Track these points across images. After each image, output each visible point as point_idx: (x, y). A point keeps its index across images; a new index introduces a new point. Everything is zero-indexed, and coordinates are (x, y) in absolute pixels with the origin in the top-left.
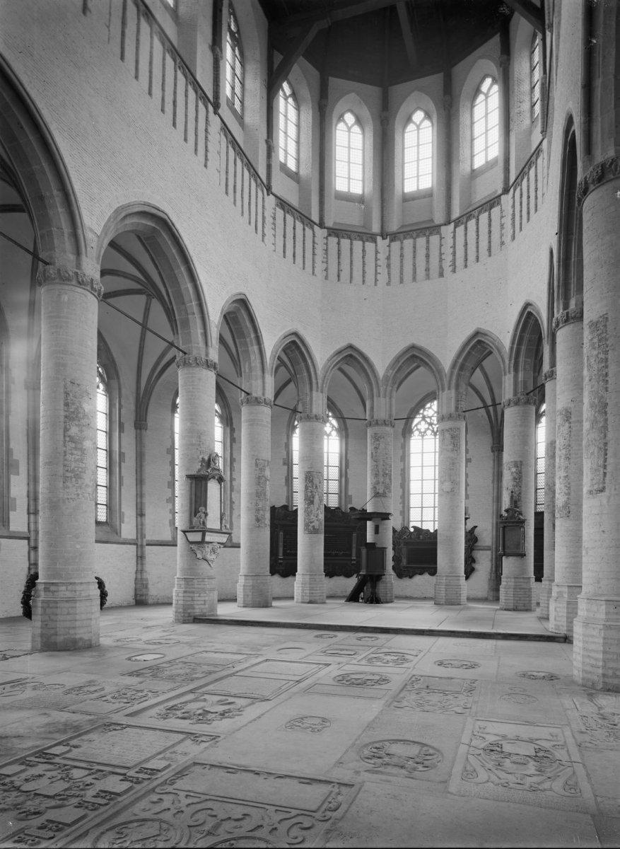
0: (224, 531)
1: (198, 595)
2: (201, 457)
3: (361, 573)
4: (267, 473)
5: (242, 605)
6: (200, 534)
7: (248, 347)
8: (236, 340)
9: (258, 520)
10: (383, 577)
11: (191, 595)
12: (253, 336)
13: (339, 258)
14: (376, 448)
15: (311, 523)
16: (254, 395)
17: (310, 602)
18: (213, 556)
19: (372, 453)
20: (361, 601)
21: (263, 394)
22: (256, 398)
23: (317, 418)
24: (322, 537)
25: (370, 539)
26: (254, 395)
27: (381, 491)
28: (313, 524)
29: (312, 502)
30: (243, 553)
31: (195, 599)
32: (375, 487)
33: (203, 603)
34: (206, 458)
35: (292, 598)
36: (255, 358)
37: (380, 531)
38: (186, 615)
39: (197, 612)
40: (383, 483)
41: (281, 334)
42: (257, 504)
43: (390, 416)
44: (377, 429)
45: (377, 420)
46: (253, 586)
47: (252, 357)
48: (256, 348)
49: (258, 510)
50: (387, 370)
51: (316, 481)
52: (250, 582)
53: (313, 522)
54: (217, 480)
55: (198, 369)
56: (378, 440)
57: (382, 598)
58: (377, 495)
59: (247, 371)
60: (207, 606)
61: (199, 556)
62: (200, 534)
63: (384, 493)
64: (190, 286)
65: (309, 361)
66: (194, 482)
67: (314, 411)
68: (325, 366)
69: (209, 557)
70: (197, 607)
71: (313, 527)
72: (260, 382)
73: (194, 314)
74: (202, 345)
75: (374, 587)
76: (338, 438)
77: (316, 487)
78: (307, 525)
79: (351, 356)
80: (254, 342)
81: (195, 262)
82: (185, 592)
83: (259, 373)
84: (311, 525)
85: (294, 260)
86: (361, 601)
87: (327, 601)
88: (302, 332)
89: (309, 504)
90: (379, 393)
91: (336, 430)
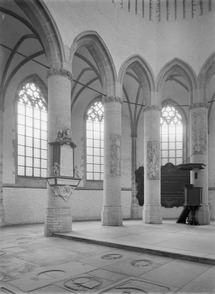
0: (76, 177)
1: (55, 219)
2: (58, 131)
3: (184, 205)
4: (118, 143)
5: (103, 225)
6: (54, 179)
7: (104, 67)
8: (98, 64)
9: (111, 172)
10: (200, 207)
11: (51, 218)
12: (106, 59)
13: (167, 7)
14: (195, 122)
15: (151, 173)
16: (109, 95)
17: (151, 223)
18: (66, 194)
19: (192, 126)
20: (187, 222)
21: (115, 95)
22: (110, 97)
23: (154, 108)
24: (159, 182)
25: (192, 182)
26: (109, 95)
27: (199, 150)
28: (152, 174)
29: (151, 160)
30: (104, 191)
31: (53, 221)
32: (194, 148)
33: (58, 224)
34: (61, 132)
35: (141, 219)
36: (109, 73)
37: (198, 177)
38: (49, 231)
39: (55, 229)
40: (200, 145)
41: (126, 57)
42: (111, 162)
43: (204, 100)
44: (195, 110)
45: (195, 104)
46: (108, 213)
47: (107, 73)
48: (109, 66)
49: (111, 166)
50: (202, 70)
51: (154, 147)
52: (107, 210)
53: (152, 172)
54: (69, 145)
55: (56, 76)
56: (196, 117)
57: (199, 221)
58: (196, 153)
59: (105, 82)
60: (61, 226)
61: (56, 194)
62: (54, 179)
63: (201, 151)
64: (47, 24)
65: (148, 73)
66: (52, 147)
67: (152, 103)
68: (159, 75)
69: (62, 194)
70: (54, 226)
71: (152, 175)
72: (112, 87)
73: (52, 42)
74: (58, 61)
75: (194, 214)
76: (181, 125)
77: (154, 150)
78: (148, 175)
79: (177, 66)
80: (107, 63)
81: (48, 8)
82: (48, 217)
83: (112, 82)
84: (151, 174)
85: (129, 8)
86: (187, 222)
87: (164, 222)
88: (142, 55)
89: (149, 162)
90: (196, 86)
91: (181, 120)
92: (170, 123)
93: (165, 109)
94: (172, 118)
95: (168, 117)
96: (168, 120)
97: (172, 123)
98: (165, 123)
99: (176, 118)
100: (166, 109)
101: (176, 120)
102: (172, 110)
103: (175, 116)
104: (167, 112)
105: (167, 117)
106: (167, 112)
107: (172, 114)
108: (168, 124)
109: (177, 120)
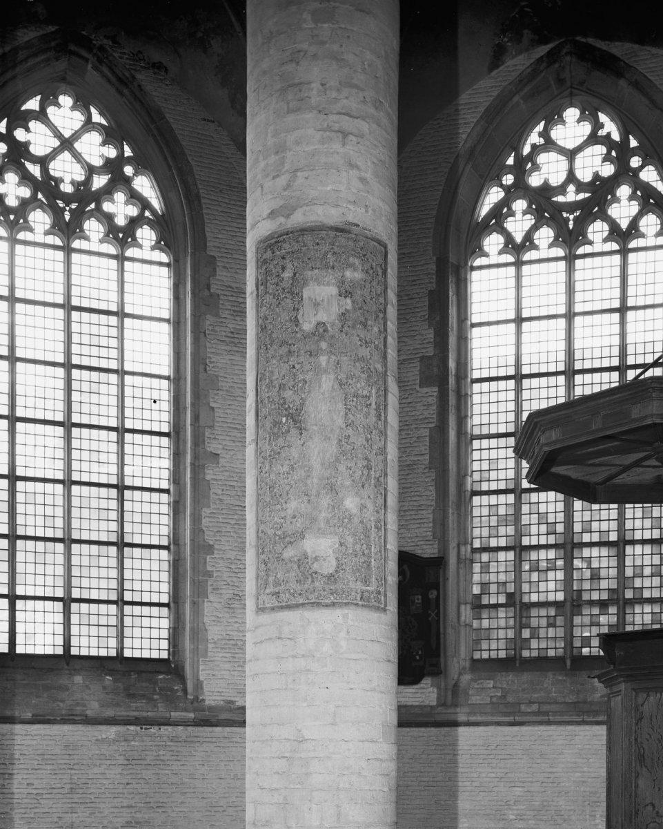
92: (584, 235)
93: (545, 134)
94: (601, 191)
95: (571, 188)
96: (571, 207)
97: (598, 230)
98: (545, 235)
99: (624, 191)
100: (557, 133)
101: (623, 209)
102: (602, 133)
103: (625, 173)
104: (562, 151)
105: (562, 189)
106: (562, 151)
107: (593, 164)
108: (571, 239)
109: (634, 208)
